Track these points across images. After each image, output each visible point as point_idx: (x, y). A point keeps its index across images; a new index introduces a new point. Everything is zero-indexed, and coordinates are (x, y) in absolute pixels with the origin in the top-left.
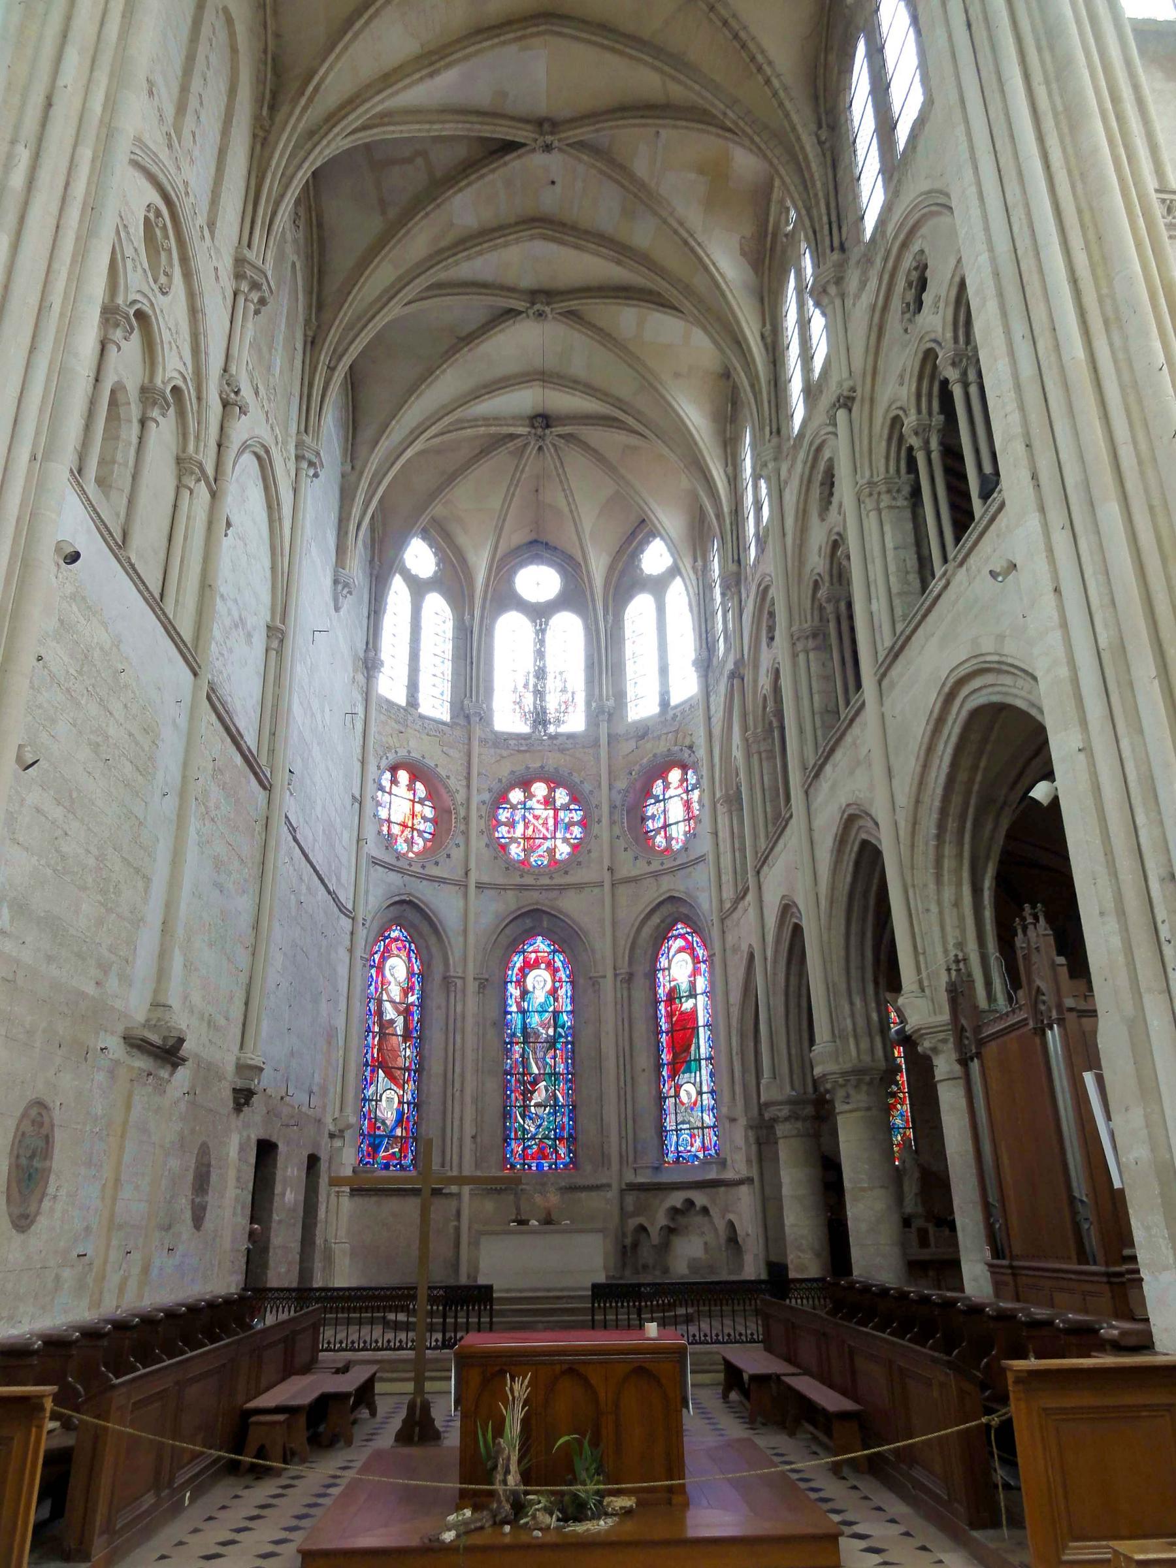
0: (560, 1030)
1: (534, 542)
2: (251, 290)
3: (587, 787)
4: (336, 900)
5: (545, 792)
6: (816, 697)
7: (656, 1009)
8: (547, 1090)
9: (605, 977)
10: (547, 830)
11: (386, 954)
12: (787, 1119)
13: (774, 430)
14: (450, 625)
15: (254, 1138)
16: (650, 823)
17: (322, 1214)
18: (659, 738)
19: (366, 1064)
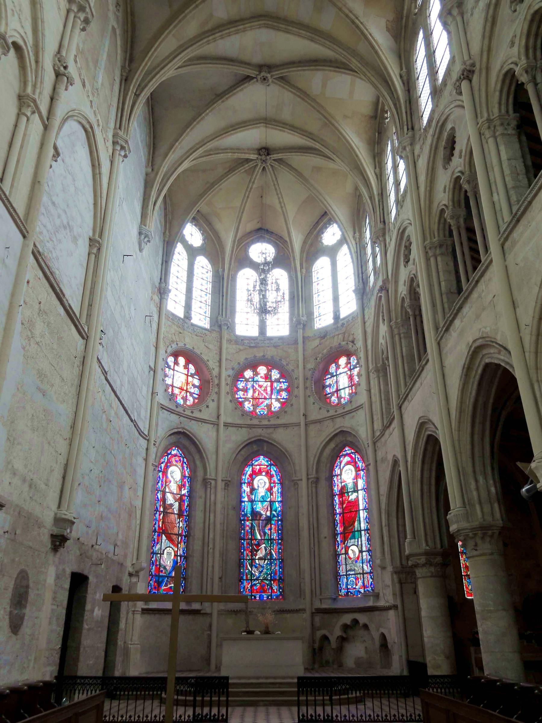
0: (274, 513)
1: (260, 229)
2: (79, 10)
3: (290, 367)
4: (136, 426)
5: (265, 372)
6: (443, 284)
7: (333, 500)
8: (266, 550)
9: (301, 480)
10: (267, 393)
11: (168, 464)
12: (424, 565)
13: (410, 127)
14: (210, 274)
15: (68, 572)
16: (328, 390)
17: (122, 625)
18: (334, 337)
19: (155, 531)
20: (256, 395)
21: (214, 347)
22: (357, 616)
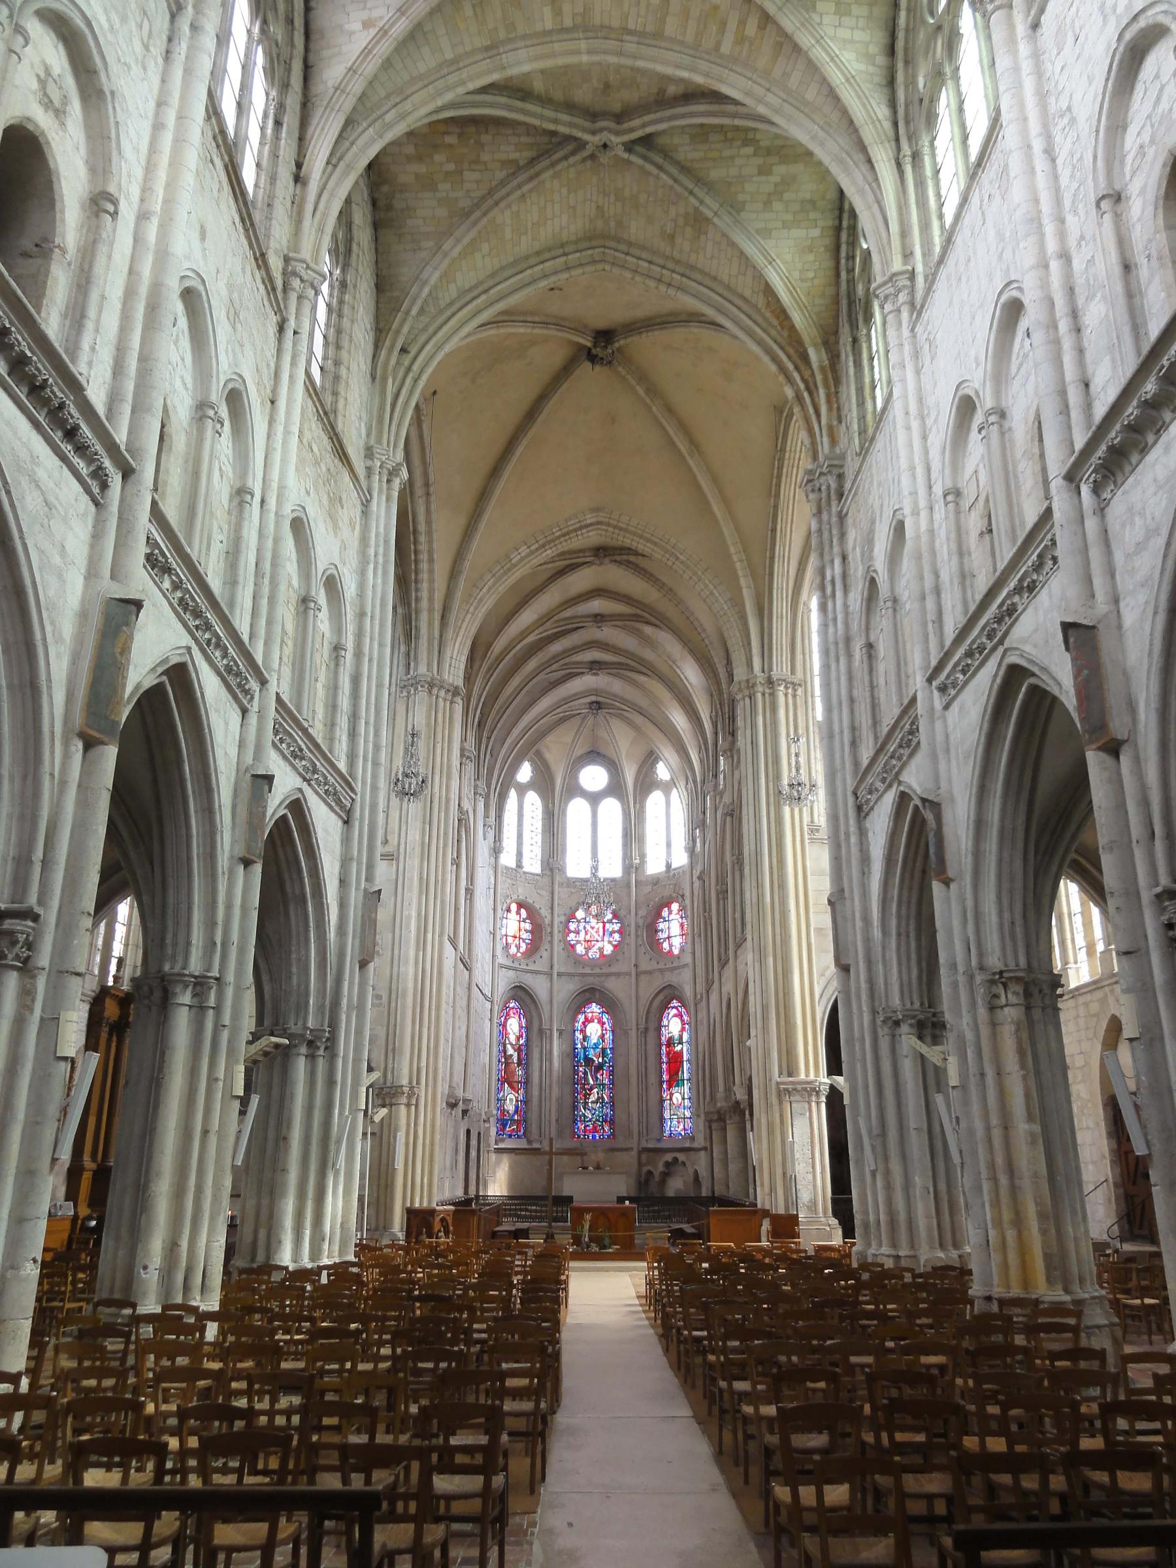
12: (716, 1121)
14: (540, 809)
22: (678, 1155)
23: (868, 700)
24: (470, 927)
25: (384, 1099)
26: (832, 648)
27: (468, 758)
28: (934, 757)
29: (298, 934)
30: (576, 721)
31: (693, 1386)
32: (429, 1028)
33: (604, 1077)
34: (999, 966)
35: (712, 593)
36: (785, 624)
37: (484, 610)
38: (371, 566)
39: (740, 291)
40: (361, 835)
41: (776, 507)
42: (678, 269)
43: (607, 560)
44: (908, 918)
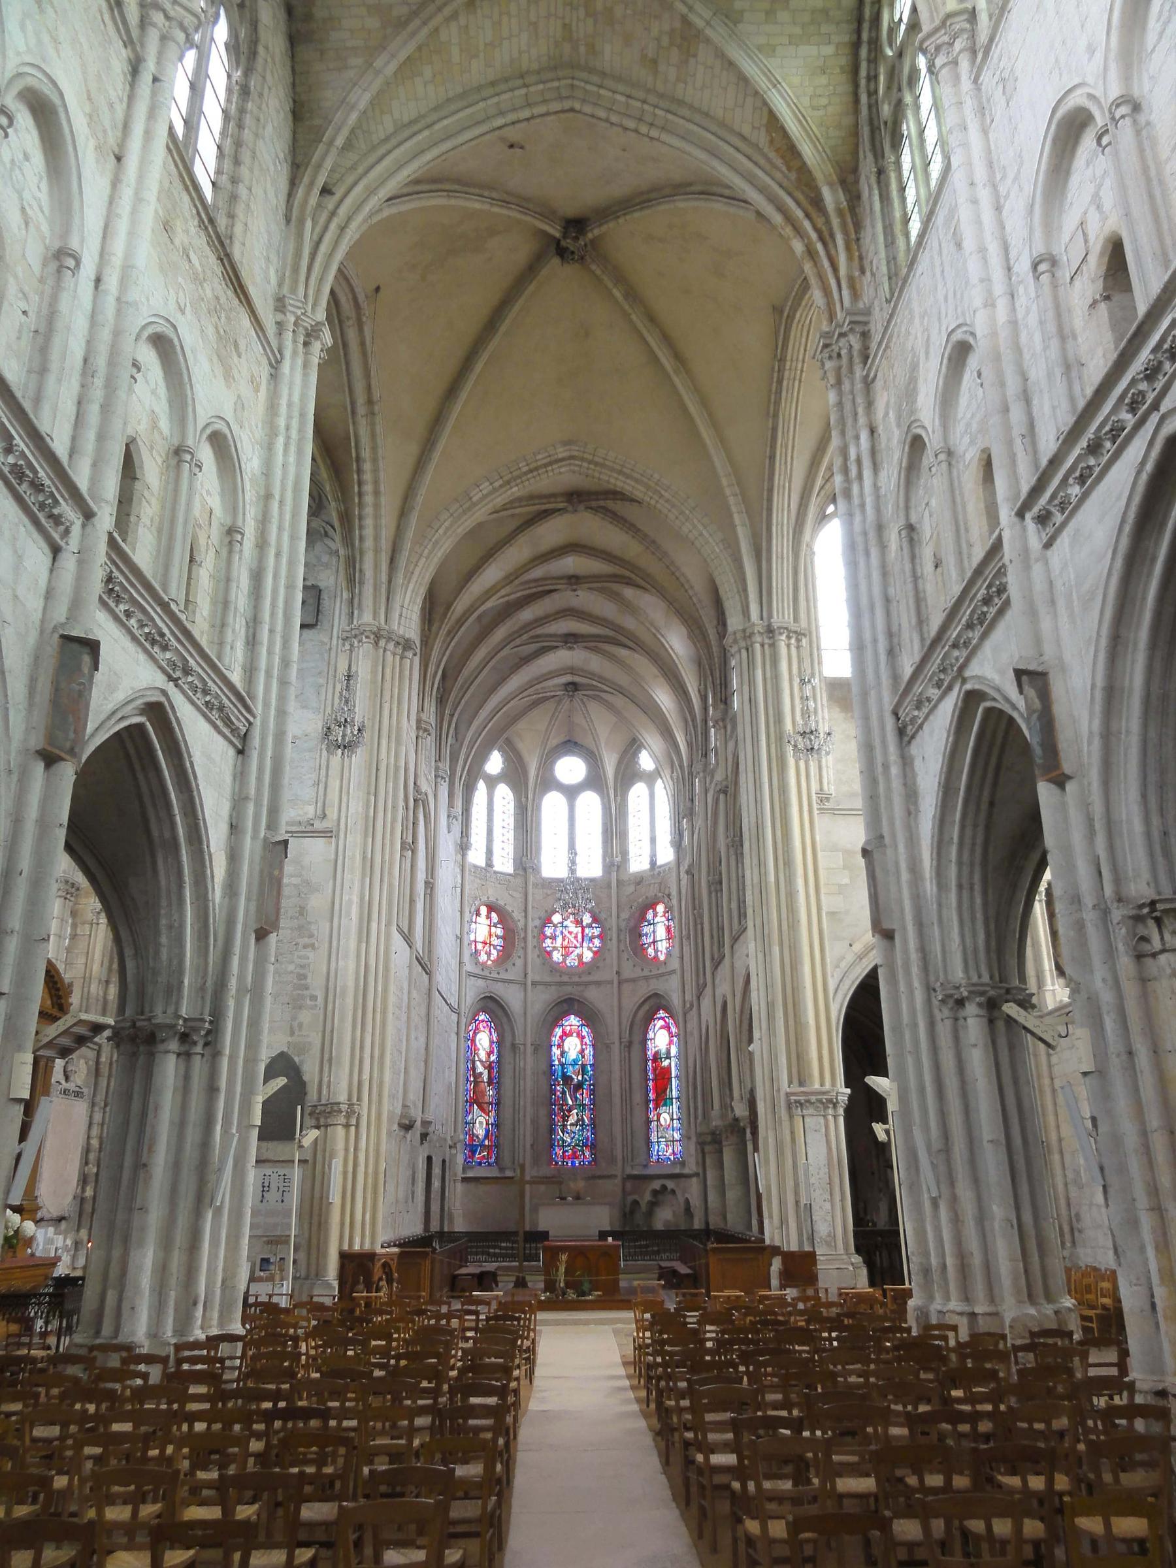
12: (710, 1143)
20: (566, 943)
21: (519, 896)
23: (911, 594)
24: (430, 926)
25: (318, 1119)
26: (859, 539)
27: (426, 730)
28: (1032, 613)
29: (169, 891)
30: (550, 705)
31: (714, 1549)
32: (373, 1034)
33: (584, 1097)
34: (1149, 894)
35: (701, 534)
36: (788, 566)
37: (440, 554)
38: (281, 440)
39: (736, 127)
40: (261, 769)
41: (774, 429)
42: (661, 104)
43: (581, 507)
44: (972, 864)
